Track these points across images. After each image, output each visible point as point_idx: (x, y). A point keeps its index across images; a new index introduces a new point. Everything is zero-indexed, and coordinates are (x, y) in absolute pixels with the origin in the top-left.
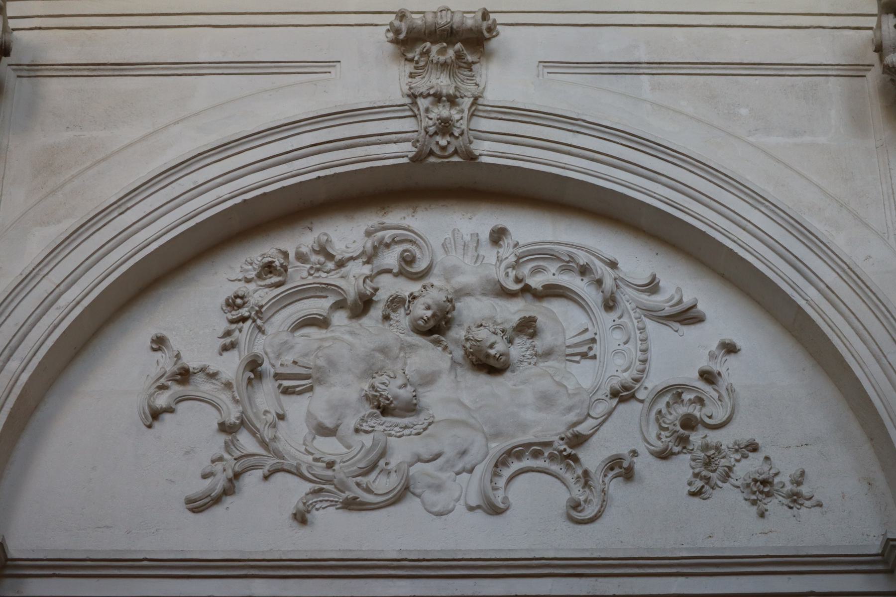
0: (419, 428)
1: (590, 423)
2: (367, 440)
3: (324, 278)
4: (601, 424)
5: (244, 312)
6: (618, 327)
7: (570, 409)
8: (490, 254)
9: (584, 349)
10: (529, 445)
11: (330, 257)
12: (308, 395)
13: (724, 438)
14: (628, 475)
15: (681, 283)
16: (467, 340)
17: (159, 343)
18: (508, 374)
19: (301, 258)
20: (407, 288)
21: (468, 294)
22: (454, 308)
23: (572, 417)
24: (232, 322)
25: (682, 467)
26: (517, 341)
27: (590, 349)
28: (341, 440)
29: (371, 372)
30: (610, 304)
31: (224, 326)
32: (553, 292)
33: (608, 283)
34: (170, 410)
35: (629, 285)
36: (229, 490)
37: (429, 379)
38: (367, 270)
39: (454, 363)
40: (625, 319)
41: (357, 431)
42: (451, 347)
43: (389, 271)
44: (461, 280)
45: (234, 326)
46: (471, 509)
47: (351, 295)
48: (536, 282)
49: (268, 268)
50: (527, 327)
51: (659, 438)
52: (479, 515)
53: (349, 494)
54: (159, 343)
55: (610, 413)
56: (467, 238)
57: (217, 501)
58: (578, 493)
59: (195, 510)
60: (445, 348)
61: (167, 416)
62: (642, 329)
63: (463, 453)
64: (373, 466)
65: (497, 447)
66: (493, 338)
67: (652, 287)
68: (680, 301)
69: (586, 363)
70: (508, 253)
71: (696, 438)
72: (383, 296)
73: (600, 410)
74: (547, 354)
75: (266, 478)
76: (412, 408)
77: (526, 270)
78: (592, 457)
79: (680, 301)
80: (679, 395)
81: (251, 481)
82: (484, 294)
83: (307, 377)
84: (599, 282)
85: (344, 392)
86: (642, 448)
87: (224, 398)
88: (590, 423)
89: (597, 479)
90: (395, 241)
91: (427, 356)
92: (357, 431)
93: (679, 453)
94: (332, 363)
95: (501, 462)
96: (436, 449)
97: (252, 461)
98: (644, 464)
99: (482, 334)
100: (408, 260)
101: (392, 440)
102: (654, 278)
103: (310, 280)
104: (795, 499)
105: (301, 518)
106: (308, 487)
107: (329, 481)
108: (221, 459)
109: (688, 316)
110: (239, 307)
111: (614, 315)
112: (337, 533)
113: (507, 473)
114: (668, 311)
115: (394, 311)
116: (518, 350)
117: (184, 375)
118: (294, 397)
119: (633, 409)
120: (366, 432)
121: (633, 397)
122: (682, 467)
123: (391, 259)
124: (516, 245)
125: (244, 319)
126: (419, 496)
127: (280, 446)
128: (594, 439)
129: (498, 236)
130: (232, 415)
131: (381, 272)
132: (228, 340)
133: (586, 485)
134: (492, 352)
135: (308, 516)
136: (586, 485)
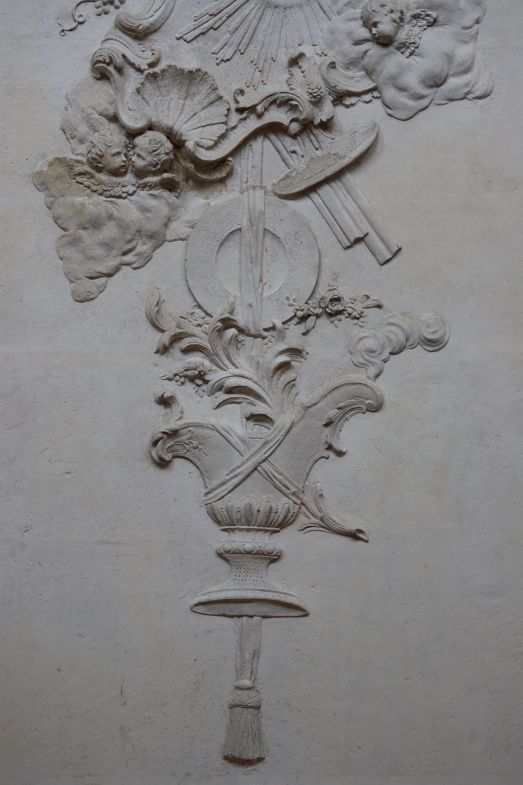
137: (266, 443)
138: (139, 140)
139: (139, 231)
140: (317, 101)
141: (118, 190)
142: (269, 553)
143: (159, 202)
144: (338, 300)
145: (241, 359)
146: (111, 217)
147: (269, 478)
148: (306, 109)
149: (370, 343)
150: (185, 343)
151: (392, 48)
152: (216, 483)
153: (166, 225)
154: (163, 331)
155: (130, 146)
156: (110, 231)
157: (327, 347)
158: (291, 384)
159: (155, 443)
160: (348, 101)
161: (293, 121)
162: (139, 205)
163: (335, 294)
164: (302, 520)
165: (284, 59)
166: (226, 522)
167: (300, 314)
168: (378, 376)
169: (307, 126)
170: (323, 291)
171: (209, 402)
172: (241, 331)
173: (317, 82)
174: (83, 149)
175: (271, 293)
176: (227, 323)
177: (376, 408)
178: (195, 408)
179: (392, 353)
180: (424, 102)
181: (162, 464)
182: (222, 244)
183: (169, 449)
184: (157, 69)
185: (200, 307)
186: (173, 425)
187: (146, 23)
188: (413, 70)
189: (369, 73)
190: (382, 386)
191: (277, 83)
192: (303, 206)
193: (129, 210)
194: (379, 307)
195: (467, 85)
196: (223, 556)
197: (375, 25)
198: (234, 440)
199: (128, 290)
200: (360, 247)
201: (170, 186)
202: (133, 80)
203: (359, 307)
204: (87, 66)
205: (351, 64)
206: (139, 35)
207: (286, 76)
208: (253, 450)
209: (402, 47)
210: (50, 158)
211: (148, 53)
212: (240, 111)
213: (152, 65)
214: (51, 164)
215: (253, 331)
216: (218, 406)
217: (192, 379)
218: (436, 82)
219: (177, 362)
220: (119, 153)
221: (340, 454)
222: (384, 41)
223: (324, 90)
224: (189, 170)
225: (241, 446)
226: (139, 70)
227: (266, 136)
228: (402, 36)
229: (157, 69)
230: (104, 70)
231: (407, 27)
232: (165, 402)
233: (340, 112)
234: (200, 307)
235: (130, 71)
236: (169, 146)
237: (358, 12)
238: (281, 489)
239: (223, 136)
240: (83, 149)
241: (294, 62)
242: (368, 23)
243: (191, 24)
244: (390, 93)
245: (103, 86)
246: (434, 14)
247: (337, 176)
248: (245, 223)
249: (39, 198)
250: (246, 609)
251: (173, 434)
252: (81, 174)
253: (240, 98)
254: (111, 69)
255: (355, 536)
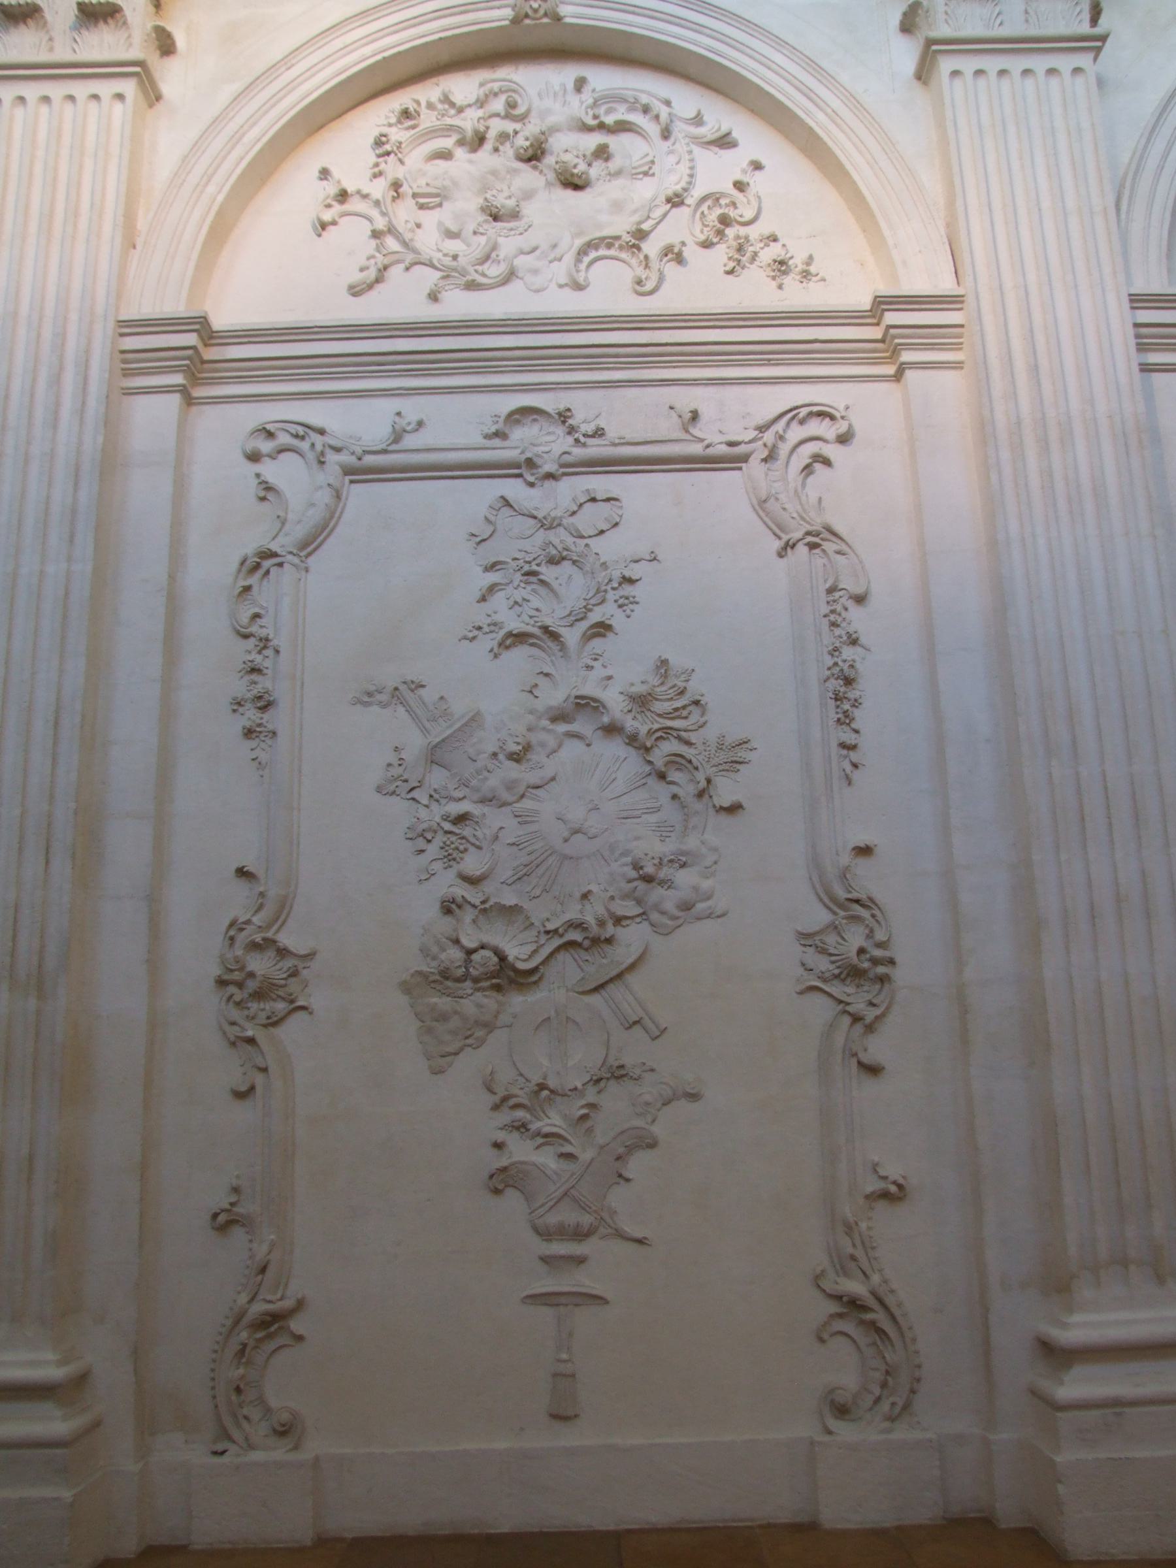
0: (521, 230)
1: (650, 223)
2: (482, 240)
3: (449, 121)
4: (658, 223)
5: (388, 147)
6: (671, 152)
7: (635, 211)
8: (574, 100)
9: (646, 168)
10: (603, 239)
11: (452, 105)
12: (439, 209)
13: (754, 232)
14: (679, 259)
15: (720, 116)
16: (557, 163)
17: (325, 174)
18: (588, 190)
19: (430, 106)
20: (510, 126)
21: (558, 130)
22: (547, 140)
23: (636, 218)
24: (379, 156)
25: (721, 254)
26: (595, 164)
27: (650, 168)
28: (464, 241)
29: (485, 188)
30: (666, 134)
31: (374, 159)
32: (623, 127)
33: (664, 117)
34: (334, 223)
35: (681, 119)
36: (378, 280)
37: (528, 195)
38: (480, 113)
39: (549, 184)
40: (677, 146)
41: (475, 233)
42: (545, 171)
43: (497, 115)
44: (552, 120)
45: (381, 160)
46: (561, 286)
47: (469, 133)
48: (609, 120)
49: (406, 114)
50: (602, 153)
51: (702, 232)
52: (567, 290)
53: (469, 278)
54: (325, 174)
55: (665, 215)
56: (557, 88)
57: (370, 287)
58: (640, 272)
59: (355, 295)
60: (541, 172)
61: (331, 228)
62: (690, 152)
63: (555, 246)
64: (487, 258)
65: (579, 242)
66: (576, 161)
67: (698, 120)
68: (719, 129)
69: (646, 179)
70: (587, 97)
71: (730, 232)
72: (491, 135)
73: (657, 214)
74: (618, 173)
75: (407, 269)
76: (515, 215)
77: (601, 111)
78: (651, 247)
79: (719, 129)
80: (718, 199)
81: (396, 271)
82: (570, 130)
83: (437, 195)
84: (657, 117)
85: (465, 206)
86: (690, 241)
87: (375, 213)
88: (650, 223)
89: (655, 264)
90: (501, 91)
91: (528, 177)
92: (475, 233)
93: (718, 243)
94: (455, 184)
95: (582, 252)
96: (534, 244)
97: (396, 257)
98: (691, 252)
99: (567, 157)
100: (512, 105)
101: (501, 240)
102: (699, 113)
103: (439, 123)
104: (806, 275)
105: (434, 297)
106: (439, 274)
107: (455, 270)
108: (373, 257)
109: (724, 142)
110: (384, 144)
111: (669, 143)
112: (459, 304)
113: (586, 260)
114: (710, 137)
115: (502, 144)
116: (594, 172)
117: (343, 196)
118: (428, 212)
119: (683, 213)
120: (482, 234)
121: (682, 203)
122: (721, 254)
123: (498, 105)
124: (594, 90)
125: (388, 154)
126: (522, 279)
127: (418, 245)
128: (652, 235)
129: (580, 84)
130: (380, 224)
131: (491, 116)
132: (376, 170)
133: (647, 267)
134: (576, 171)
135: (439, 296)
136: (647, 267)
137: (572, 1176)
138: (475, 957)
139: (476, 1022)
140: (601, 923)
141: (460, 993)
142: (578, 1257)
143: (489, 1001)
144: (622, 1067)
145: (552, 1114)
146: (456, 1012)
147: (575, 1200)
148: (595, 930)
149: (648, 1098)
150: (512, 1102)
151: (654, 884)
152: (538, 1205)
153: (496, 1017)
154: (495, 1094)
155: (468, 961)
156: (455, 1022)
157: (616, 1104)
158: (590, 1131)
159: (491, 1176)
160: (624, 923)
161: (585, 938)
162: (475, 1003)
163: (621, 1063)
164: (602, 1231)
165: (578, 895)
166: (546, 1234)
167: (595, 1078)
168: (654, 1121)
169: (596, 941)
170: (611, 1061)
171: (529, 1144)
172: (552, 1091)
173: (601, 911)
174: (434, 964)
175: (582, 1058)
176: (542, 1087)
177: (652, 1145)
178: (521, 1150)
179: (664, 1104)
180: (681, 921)
181: (497, 1192)
182: (537, 1028)
183: (502, 1181)
184: (487, 906)
185: (521, 1075)
186: (504, 1162)
187: (478, 873)
188: (669, 899)
189: (639, 902)
190: (656, 1129)
191: (573, 913)
192: (595, 1000)
193: (468, 1006)
194: (652, 1070)
195: (710, 908)
196: (545, 1260)
197: (641, 868)
198: (548, 1172)
199: (469, 1065)
200: (637, 1028)
201: (498, 988)
202: (468, 915)
203: (638, 1071)
204: (438, 905)
205: (625, 897)
206: (472, 881)
207: (580, 907)
208: (563, 1180)
209: (662, 883)
210: (412, 971)
211: (480, 894)
212: (547, 932)
213: (483, 902)
214: (412, 975)
215: (560, 1091)
216: (537, 1148)
217: (518, 1128)
218: (686, 907)
219: (505, 1117)
220: (460, 966)
221: (628, 1180)
222: (648, 879)
223: (606, 915)
224: (508, 977)
225: (555, 1177)
226: (474, 906)
227: (566, 950)
228: (662, 875)
229: (487, 906)
230: (449, 907)
231: (665, 869)
232: (498, 1146)
233: (619, 929)
234: (521, 1075)
235: (468, 907)
236: (496, 959)
237: (629, 859)
238: (584, 1208)
239: (535, 952)
240: (434, 964)
241: (585, 896)
242: (637, 866)
243: (510, 873)
244: (655, 916)
245: (448, 919)
246: (684, 859)
247: (620, 976)
248: (553, 1013)
249: (403, 1000)
250: (563, 1300)
251: (504, 1170)
252: (434, 981)
253: (547, 924)
254: (453, 906)
255: (640, 1241)
